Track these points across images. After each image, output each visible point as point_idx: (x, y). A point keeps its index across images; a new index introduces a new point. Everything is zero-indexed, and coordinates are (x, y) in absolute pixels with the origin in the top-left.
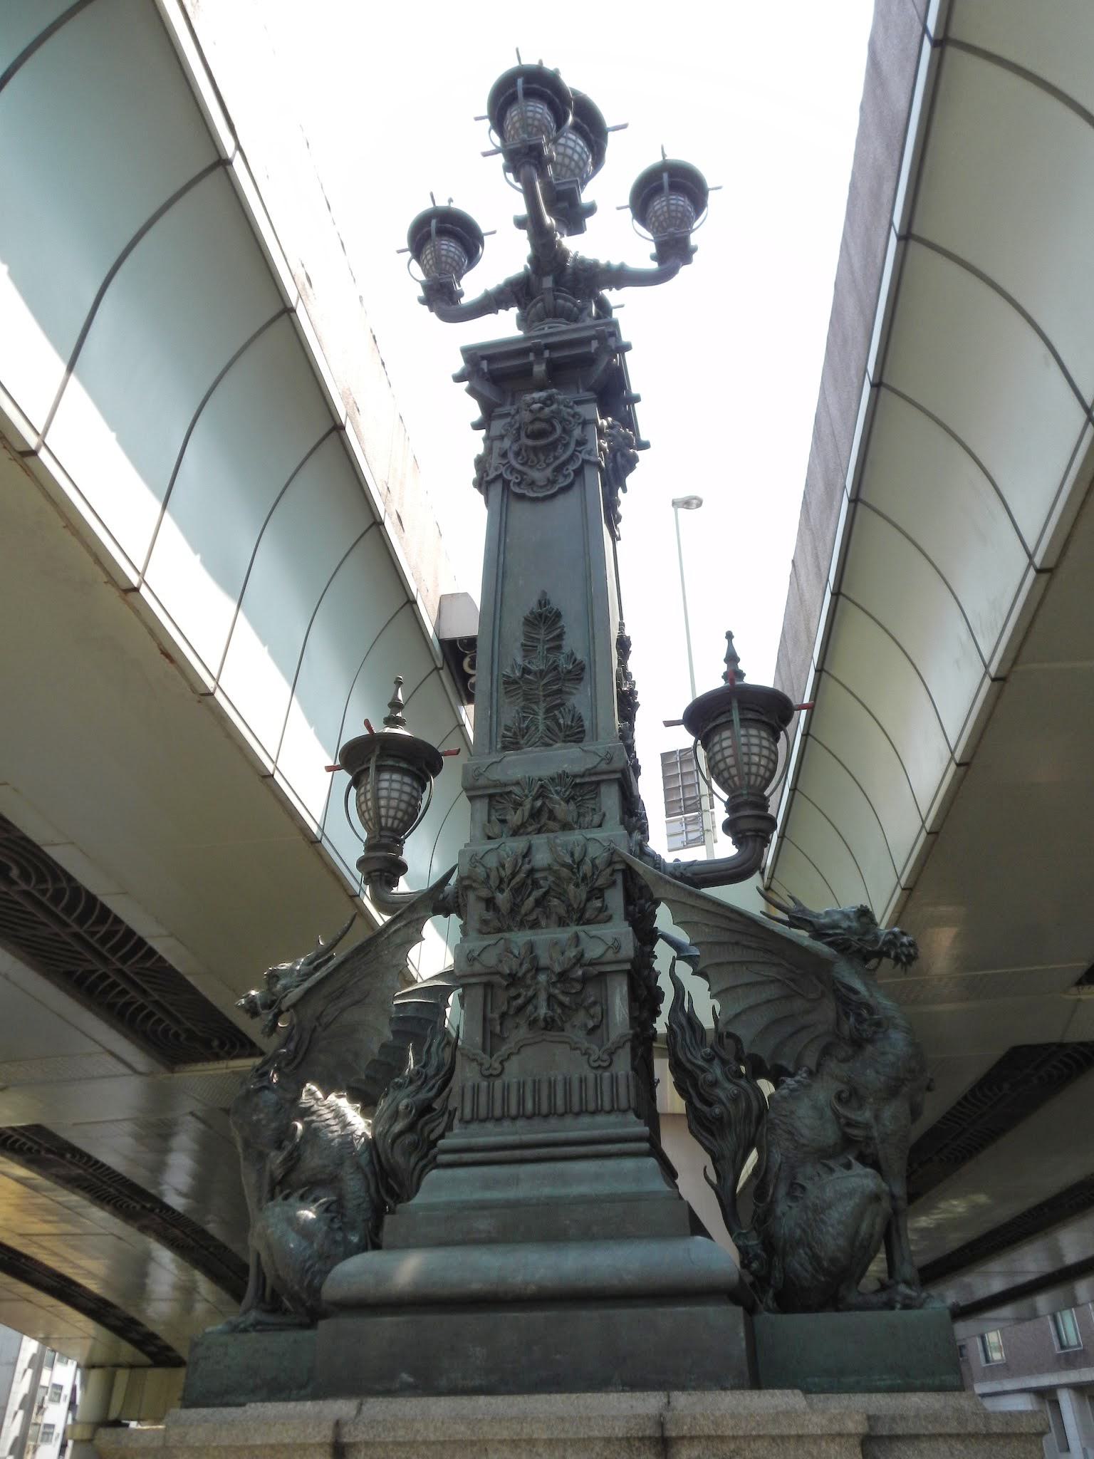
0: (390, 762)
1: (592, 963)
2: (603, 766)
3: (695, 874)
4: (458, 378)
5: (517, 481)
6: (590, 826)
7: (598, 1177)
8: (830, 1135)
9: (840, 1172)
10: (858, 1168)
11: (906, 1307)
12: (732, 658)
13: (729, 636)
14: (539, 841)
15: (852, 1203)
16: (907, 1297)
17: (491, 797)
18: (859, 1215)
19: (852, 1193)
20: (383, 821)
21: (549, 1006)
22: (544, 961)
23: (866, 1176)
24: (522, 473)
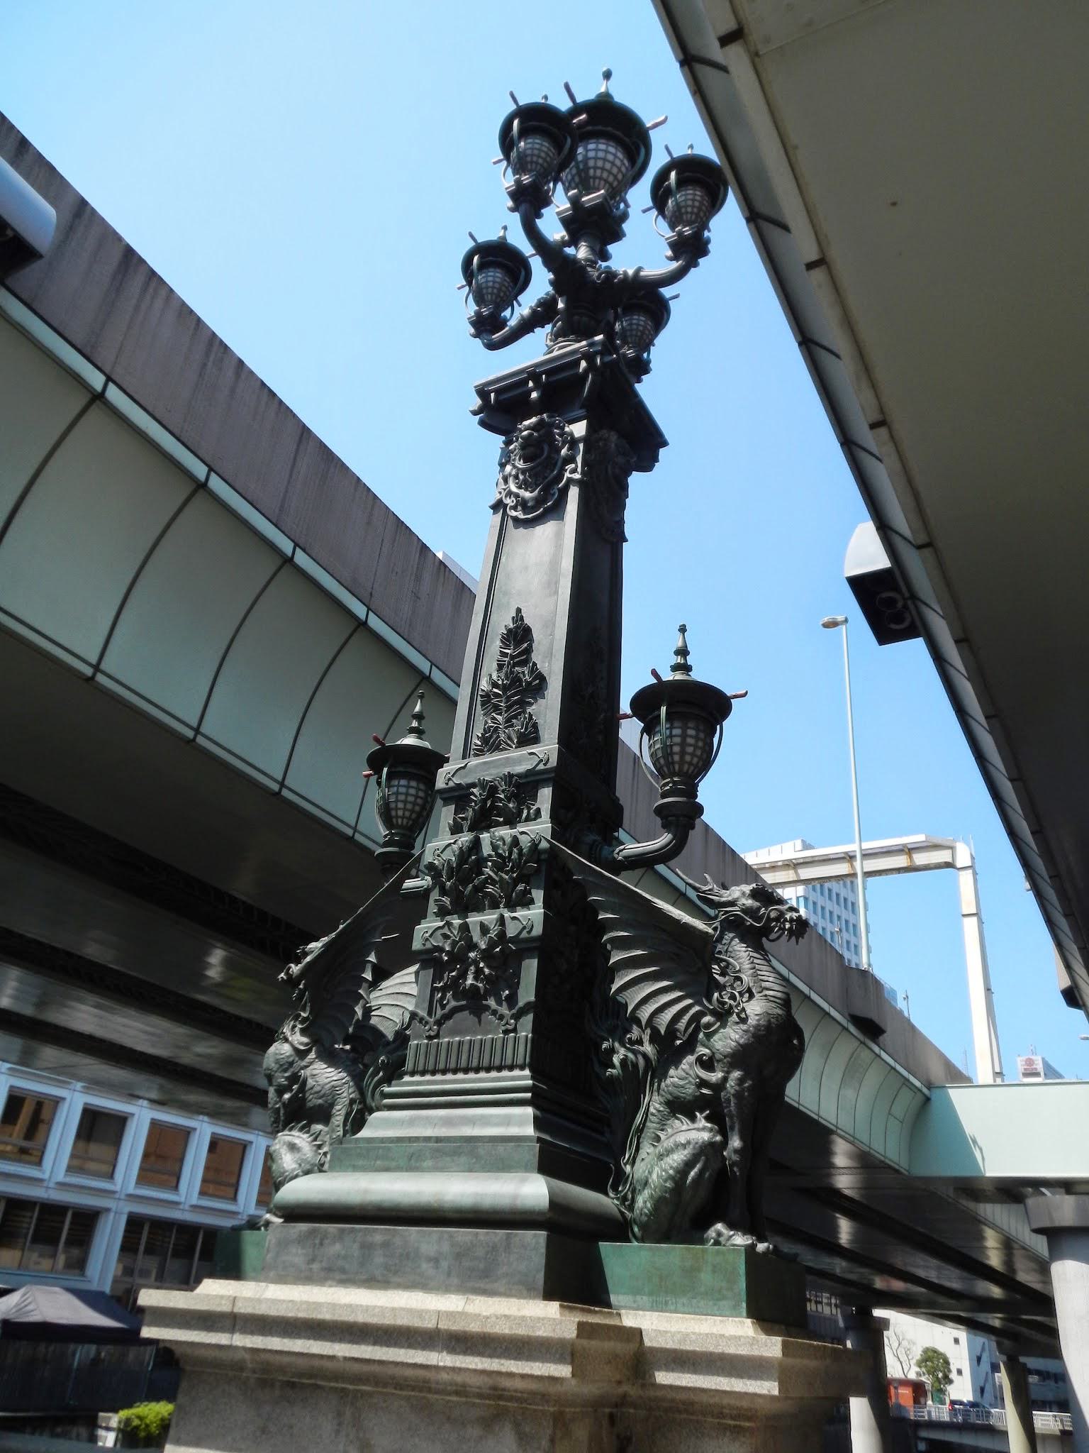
0: (401, 769)
3: (625, 857)
4: (475, 413)
5: (513, 504)
6: (528, 819)
7: (401, 1123)
12: (683, 652)
13: (683, 629)
15: (686, 1152)
16: (719, 1234)
18: (689, 1165)
19: (689, 1142)
20: (394, 820)
21: (476, 978)
23: (704, 1129)
24: (517, 496)
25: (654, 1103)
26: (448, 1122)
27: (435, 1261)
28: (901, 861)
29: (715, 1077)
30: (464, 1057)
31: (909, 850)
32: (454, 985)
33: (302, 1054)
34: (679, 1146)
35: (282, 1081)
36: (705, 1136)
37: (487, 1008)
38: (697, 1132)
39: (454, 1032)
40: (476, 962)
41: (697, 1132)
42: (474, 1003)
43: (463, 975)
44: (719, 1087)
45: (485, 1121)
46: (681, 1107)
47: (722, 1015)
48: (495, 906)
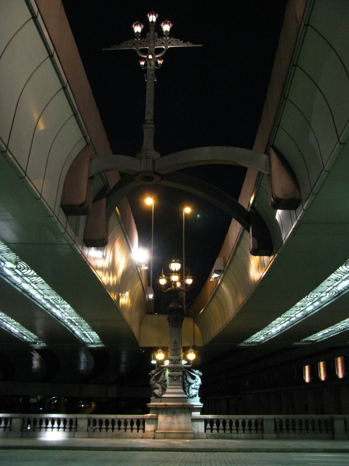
8: (194, 388)
14: (175, 365)
42: (175, 380)
43: (174, 378)
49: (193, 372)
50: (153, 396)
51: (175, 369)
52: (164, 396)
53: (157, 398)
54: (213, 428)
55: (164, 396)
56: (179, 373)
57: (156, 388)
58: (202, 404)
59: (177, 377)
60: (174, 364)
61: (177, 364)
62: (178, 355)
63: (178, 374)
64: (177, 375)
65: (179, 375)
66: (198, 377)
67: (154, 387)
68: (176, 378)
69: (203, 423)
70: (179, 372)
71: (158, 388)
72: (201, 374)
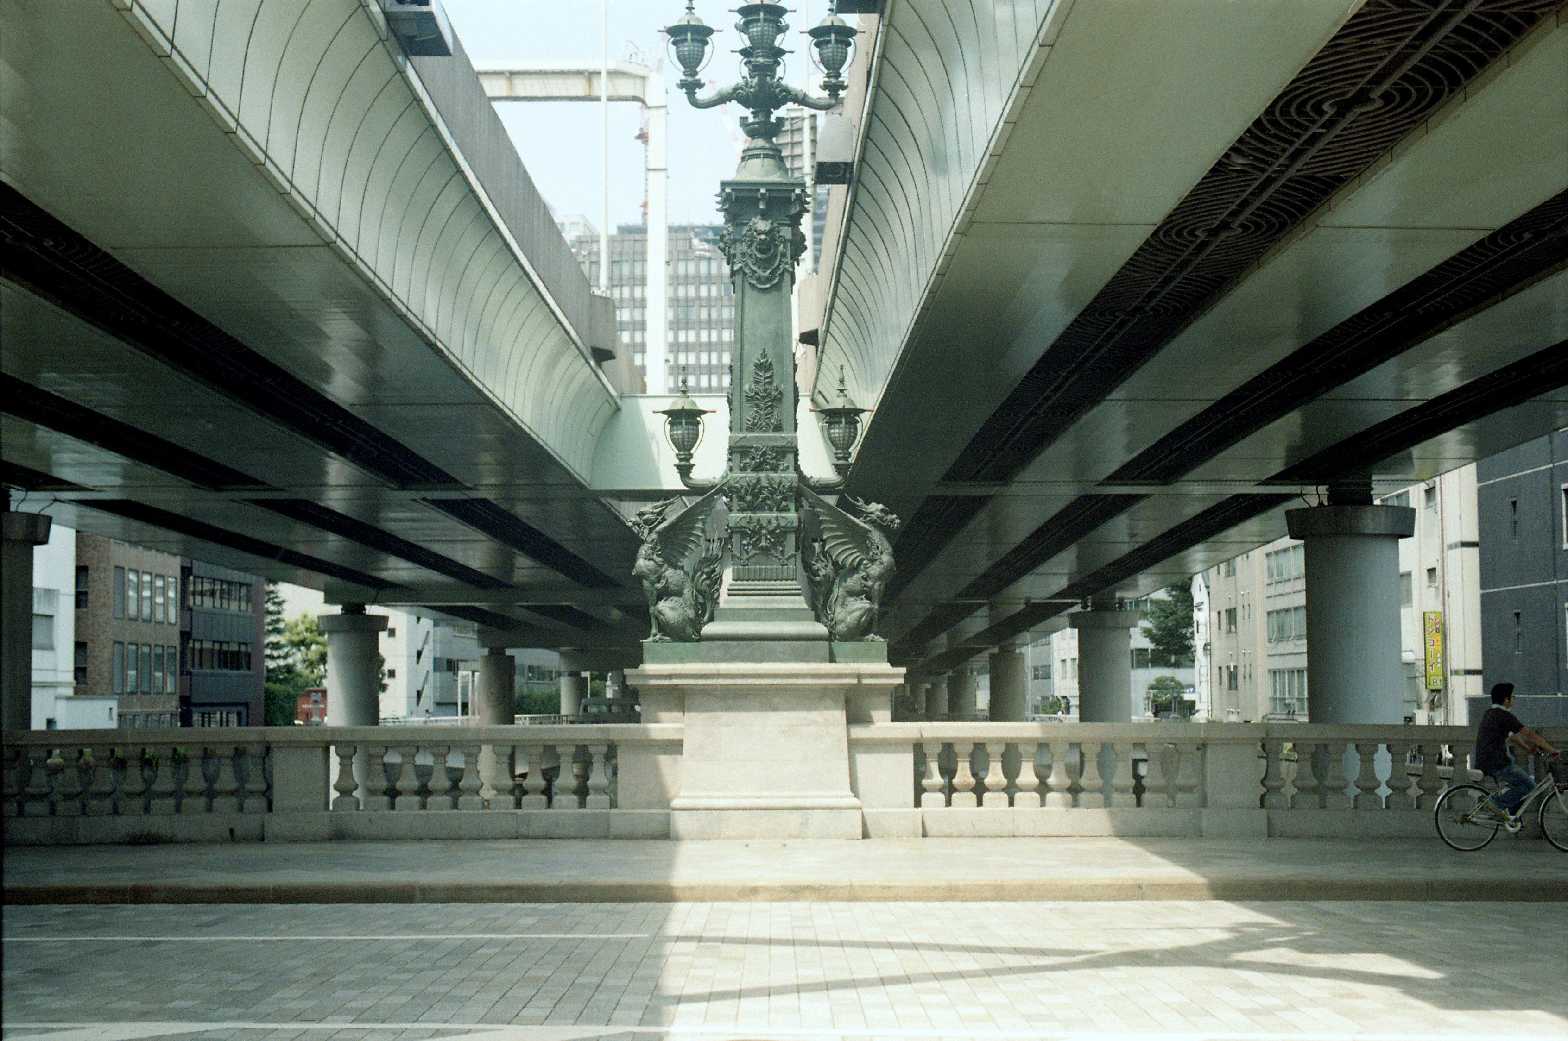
1: (783, 527)
2: (789, 445)
4: (717, 196)
9: (859, 602)
10: (865, 601)
11: (872, 641)
14: (763, 475)
17: (740, 452)
18: (862, 616)
22: (764, 524)
25: (838, 591)
26: (765, 602)
27: (783, 653)
28: (578, 87)
29: (870, 583)
30: (763, 575)
31: (591, 75)
32: (755, 545)
33: (661, 566)
34: (857, 609)
35: (653, 578)
36: (868, 606)
37: (772, 555)
38: (863, 604)
39: (755, 564)
40: (765, 535)
41: (863, 604)
42: (765, 550)
43: (759, 539)
44: (871, 588)
45: (783, 602)
46: (852, 593)
47: (872, 561)
48: (771, 509)
49: (857, 513)
50: (654, 631)
51: (765, 493)
52: (708, 629)
53: (674, 641)
54: (956, 781)
55: (708, 629)
56: (784, 515)
57: (664, 594)
58: (903, 670)
59: (771, 533)
60: (757, 468)
61: (774, 469)
62: (778, 428)
63: (777, 519)
64: (774, 523)
65: (783, 524)
66: (876, 536)
67: (659, 586)
68: (767, 539)
69: (908, 759)
70: (786, 509)
71: (679, 593)
72: (895, 520)
